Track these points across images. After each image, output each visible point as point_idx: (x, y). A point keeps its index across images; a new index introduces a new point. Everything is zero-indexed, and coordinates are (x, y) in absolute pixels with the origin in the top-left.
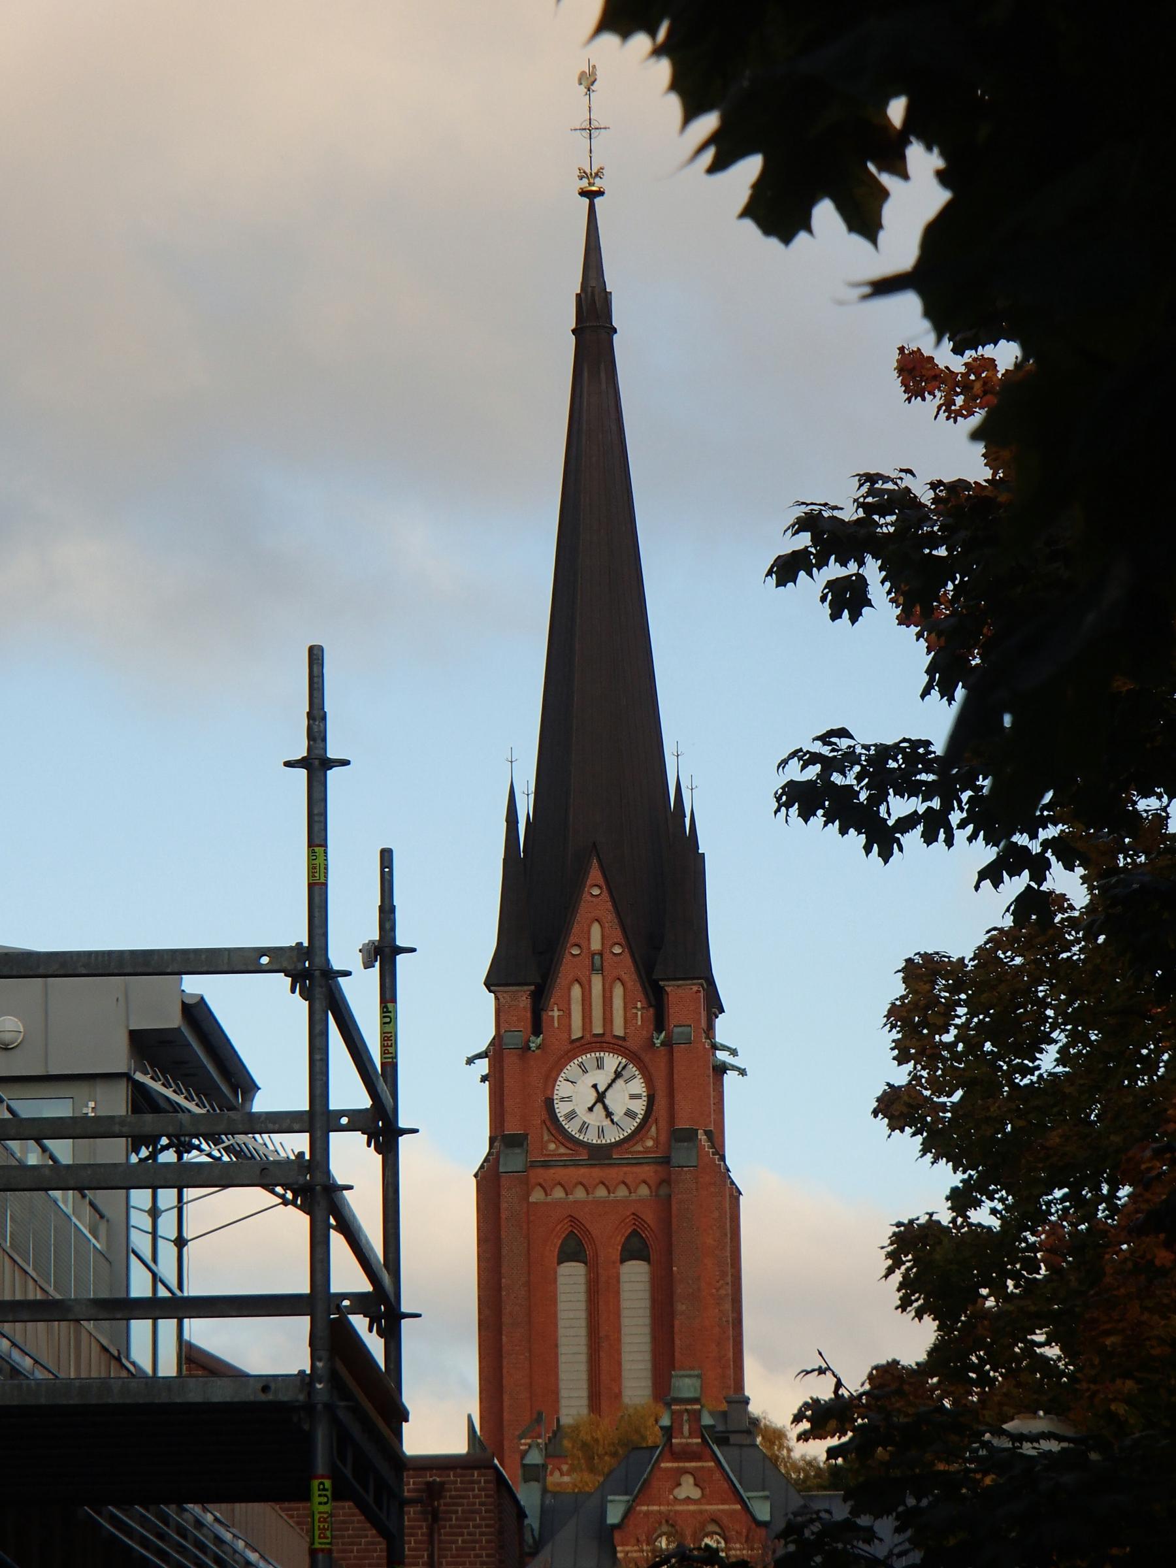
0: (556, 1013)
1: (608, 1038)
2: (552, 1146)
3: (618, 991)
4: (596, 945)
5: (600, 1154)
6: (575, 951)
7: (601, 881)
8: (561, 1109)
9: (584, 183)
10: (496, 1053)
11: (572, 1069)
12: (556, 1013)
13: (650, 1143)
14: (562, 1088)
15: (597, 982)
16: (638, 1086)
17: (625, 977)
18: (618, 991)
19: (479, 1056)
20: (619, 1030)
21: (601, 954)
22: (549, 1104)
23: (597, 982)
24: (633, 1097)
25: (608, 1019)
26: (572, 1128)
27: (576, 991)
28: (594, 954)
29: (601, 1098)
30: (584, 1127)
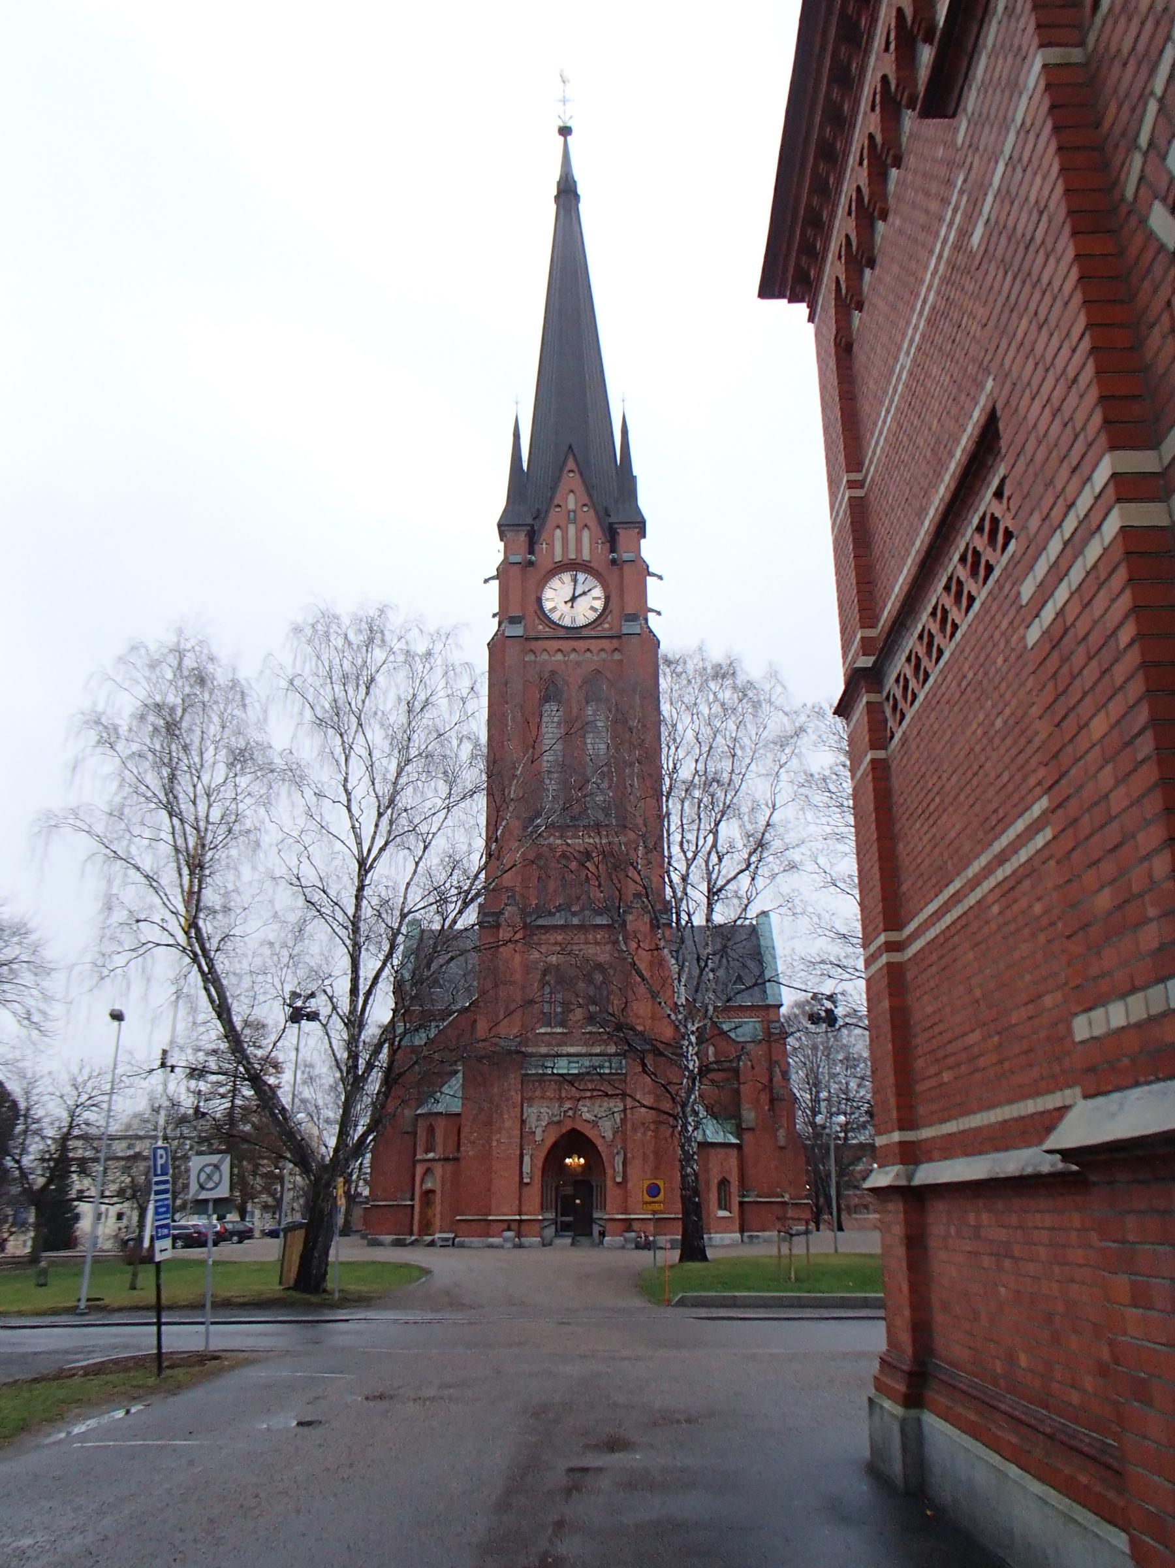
0: (544, 546)
1: (578, 561)
2: (541, 627)
3: (586, 533)
4: (571, 505)
5: (574, 633)
6: (558, 509)
7: (575, 469)
8: (548, 605)
10: (502, 574)
11: (555, 583)
12: (544, 546)
13: (606, 626)
14: (548, 594)
15: (572, 529)
16: (598, 592)
18: (586, 534)
19: (492, 578)
20: (586, 555)
21: (574, 511)
22: (539, 600)
23: (572, 529)
24: (595, 598)
25: (579, 549)
26: (555, 617)
27: (558, 533)
28: (569, 512)
29: (573, 599)
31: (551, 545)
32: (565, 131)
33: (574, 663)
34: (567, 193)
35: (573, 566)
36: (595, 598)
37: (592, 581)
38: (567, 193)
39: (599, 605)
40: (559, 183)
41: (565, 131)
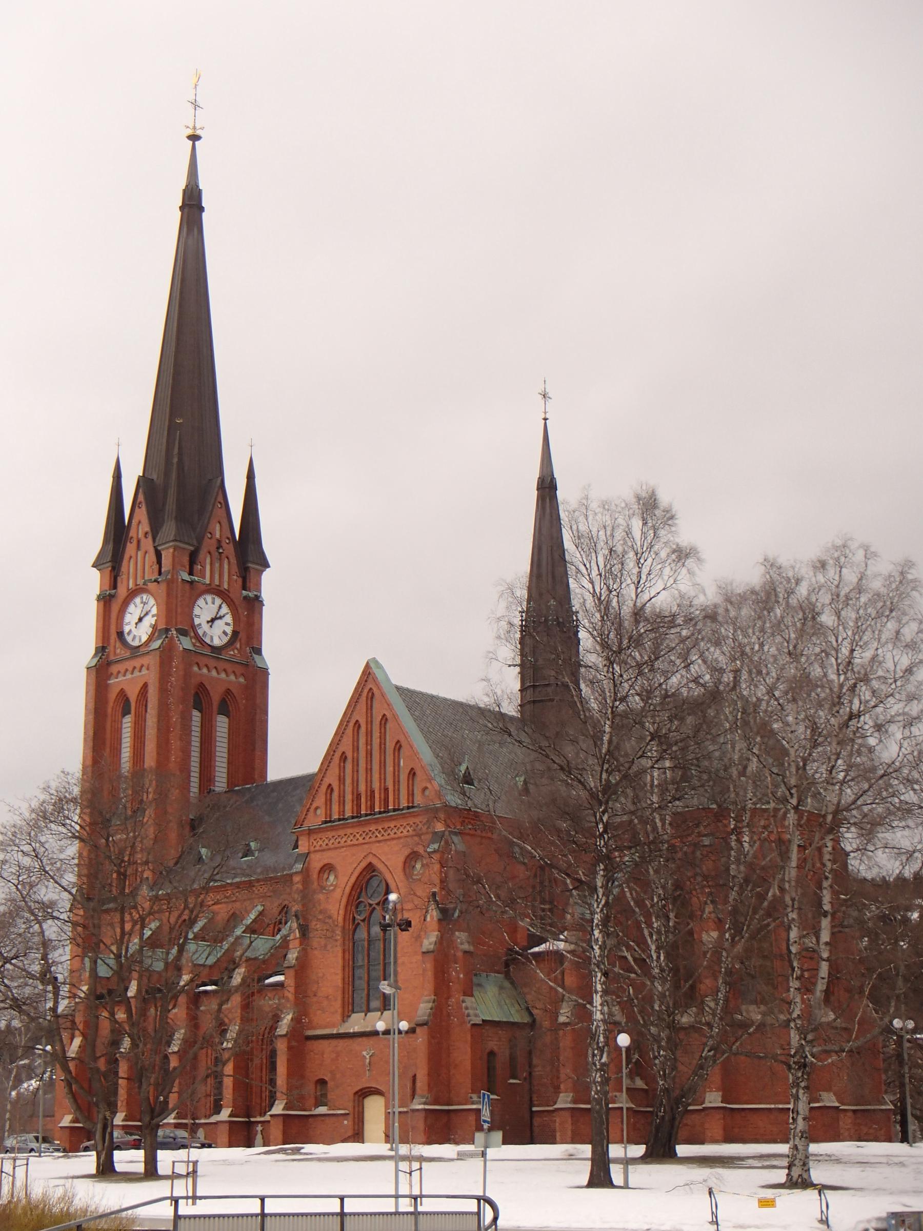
3: (226, 561)
4: (218, 536)
6: (209, 536)
8: (197, 621)
9: (190, 132)
11: (201, 602)
16: (229, 618)
17: (230, 557)
24: (227, 624)
26: (200, 632)
30: (205, 634)
31: (204, 567)
32: (194, 138)
33: (220, 679)
34: (192, 205)
35: (218, 591)
36: (227, 624)
37: (225, 609)
38: (192, 205)
39: (229, 630)
40: (184, 191)
41: (194, 138)
